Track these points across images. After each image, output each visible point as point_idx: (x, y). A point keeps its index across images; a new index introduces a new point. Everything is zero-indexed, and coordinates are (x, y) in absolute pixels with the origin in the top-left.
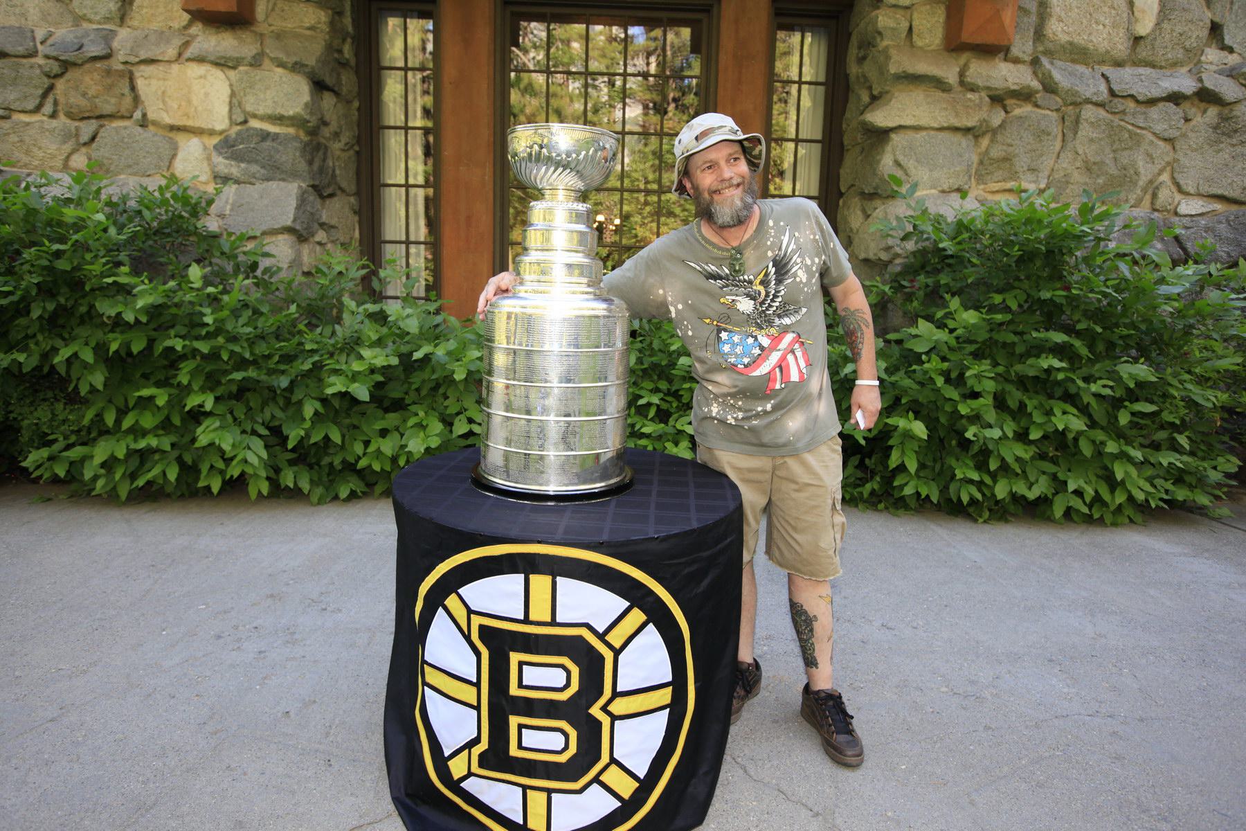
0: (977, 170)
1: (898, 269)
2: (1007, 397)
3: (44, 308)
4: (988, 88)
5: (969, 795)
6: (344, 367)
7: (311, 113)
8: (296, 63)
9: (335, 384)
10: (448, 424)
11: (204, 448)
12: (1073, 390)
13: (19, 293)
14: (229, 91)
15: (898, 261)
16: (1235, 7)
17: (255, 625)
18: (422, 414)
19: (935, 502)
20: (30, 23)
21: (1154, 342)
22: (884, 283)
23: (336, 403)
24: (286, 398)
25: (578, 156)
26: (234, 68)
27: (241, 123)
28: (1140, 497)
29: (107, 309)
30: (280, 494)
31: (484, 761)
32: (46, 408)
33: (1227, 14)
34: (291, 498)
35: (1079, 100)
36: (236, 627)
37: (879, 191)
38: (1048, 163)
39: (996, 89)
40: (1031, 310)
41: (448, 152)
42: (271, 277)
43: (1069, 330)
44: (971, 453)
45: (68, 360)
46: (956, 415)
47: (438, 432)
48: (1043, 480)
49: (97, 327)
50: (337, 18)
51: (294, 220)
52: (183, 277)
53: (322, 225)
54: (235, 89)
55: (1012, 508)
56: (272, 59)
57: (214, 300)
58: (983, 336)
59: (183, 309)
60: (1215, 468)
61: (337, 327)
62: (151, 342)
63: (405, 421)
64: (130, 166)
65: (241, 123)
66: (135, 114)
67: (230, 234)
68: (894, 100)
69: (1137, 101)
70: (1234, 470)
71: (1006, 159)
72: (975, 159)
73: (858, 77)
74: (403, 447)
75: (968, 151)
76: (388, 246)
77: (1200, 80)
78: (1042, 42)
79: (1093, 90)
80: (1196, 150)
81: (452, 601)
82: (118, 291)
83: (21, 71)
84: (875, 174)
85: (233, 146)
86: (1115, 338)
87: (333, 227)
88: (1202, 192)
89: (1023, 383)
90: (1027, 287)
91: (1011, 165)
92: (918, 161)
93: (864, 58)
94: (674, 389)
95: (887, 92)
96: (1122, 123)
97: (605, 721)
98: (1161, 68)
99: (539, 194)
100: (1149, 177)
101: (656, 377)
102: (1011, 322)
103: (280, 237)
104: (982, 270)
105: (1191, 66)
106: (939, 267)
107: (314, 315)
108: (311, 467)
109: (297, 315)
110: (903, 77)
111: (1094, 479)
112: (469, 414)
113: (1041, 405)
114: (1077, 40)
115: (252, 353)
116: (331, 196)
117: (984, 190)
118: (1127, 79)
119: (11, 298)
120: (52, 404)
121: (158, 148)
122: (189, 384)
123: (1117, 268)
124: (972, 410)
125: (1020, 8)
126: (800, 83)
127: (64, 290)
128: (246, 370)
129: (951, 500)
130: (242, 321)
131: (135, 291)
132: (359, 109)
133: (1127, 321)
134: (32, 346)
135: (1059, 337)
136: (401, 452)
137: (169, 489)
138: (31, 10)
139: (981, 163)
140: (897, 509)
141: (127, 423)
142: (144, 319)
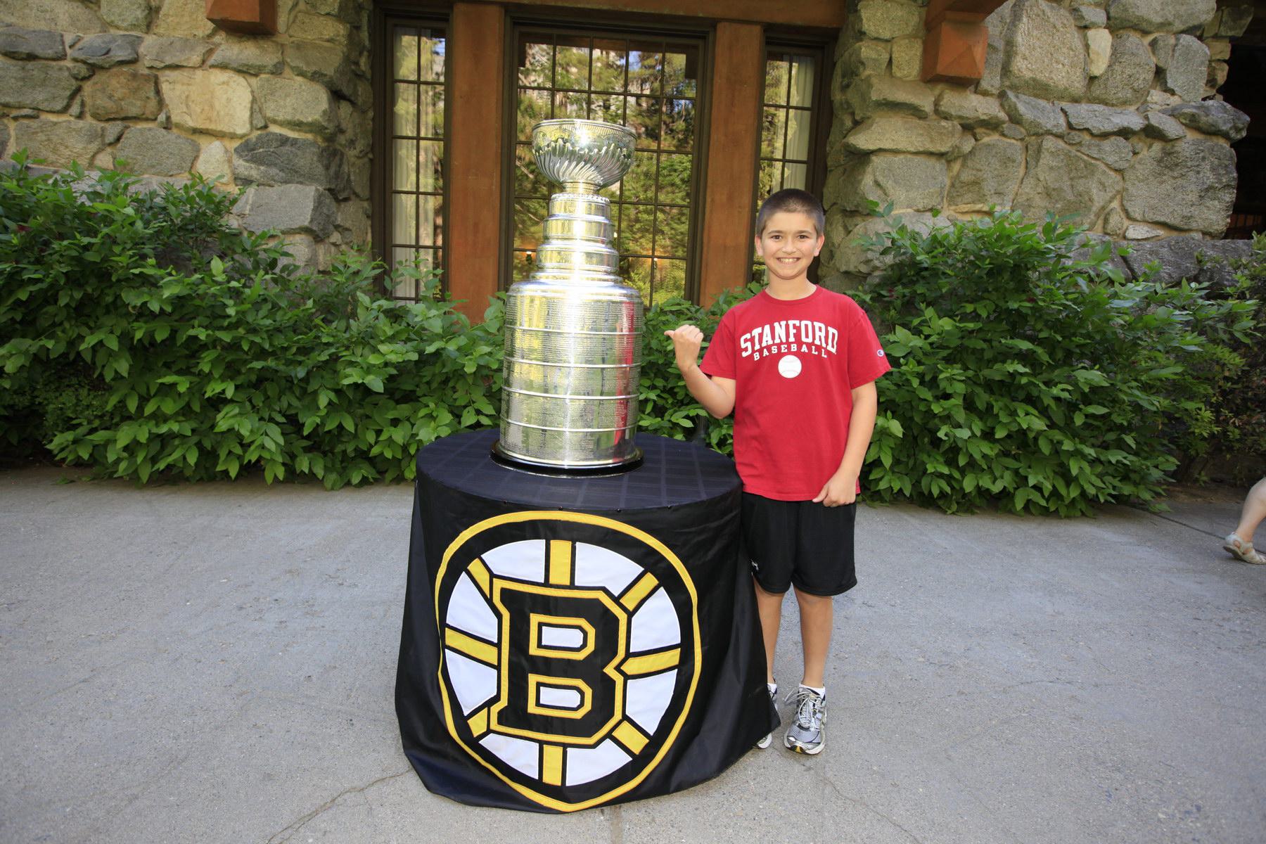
0: (949, 192)
1: (877, 280)
2: (976, 399)
3: (72, 297)
4: (960, 117)
5: (946, 751)
6: (359, 360)
7: (329, 120)
8: (315, 73)
9: (351, 375)
10: (458, 416)
11: (223, 433)
12: (1035, 393)
13: (48, 280)
14: (248, 97)
15: (877, 273)
16: (1177, 54)
17: (275, 597)
18: (432, 405)
19: (908, 495)
20: (59, 28)
21: (1107, 351)
22: (865, 292)
23: (350, 394)
24: (302, 387)
25: (600, 151)
26: (256, 75)
27: (261, 128)
28: (1092, 491)
29: (133, 299)
30: (295, 479)
31: (503, 718)
32: (71, 394)
33: (1170, 60)
34: (306, 483)
35: (1041, 131)
36: (257, 599)
37: (860, 209)
38: (1012, 187)
39: (968, 118)
40: (998, 319)
41: (457, 162)
42: (289, 275)
43: (1032, 339)
44: (942, 450)
45: (93, 347)
46: (929, 414)
47: (448, 422)
48: (1008, 476)
49: (121, 317)
50: (355, 31)
51: (311, 221)
52: (205, 268)
53: (337, 227)
54: (256, 95)
55: (978, 501)
56: (292, 68)
57: (236, 294)
58: (955, 342)
59: (206, 301)
60: (1156, 467)
61: (351, 321)
62: (174, 333)
63: (416, 412)
64: (153, 166)
65: (261, 128)
66: (159, 117)
67: (252, 233)
68: (875, 125)
69: (1092, 135)
70: (1173, 468)
71: (976, 183)
72: (948, 182)
73: (841, 104)
74: (414, 436)
75: (941, 175)
76: (398, 249)
77: (1147, 118)
78: (1008, 78)
79: (1055, 123)
80: (1143, 181)
81: (475, 566)
82: (143, 284)
83: (50, 73)
84: (856, 193)
85: (253, 150)
86: (1072, 347)
87: (347, 229)
88: (1147, 219)
89: (989, 386)
90: (994, 298)
91: (980, 188)
92: (896, 182)
93: (848, 86)
94: (670, 386)
95: (869, 118)
96: (1079, 154)
97: (619, 680)
98: (1113, 105)
99: (561, 187)
100: (1102, 204)
101: (652, 375)
102: (980, 330)
103: (298, 238)
104: (956, 282)
105: (1139, 105)
106: (915, 279)
107: (329, 312)
108: (325, 454)
109: (314, 310)
110: (884, 104)
111: (1051, 475)
112: (477, 406)
113: (1006, 406)
114: (1039, 76)
115: (271, 345)
116: (346, 200)
117: (955, 210)
118: (1084, 114)
119: (39, 286)
120: (77, 390)
121: (181, 150)
122: (210, 372)
123: (1076, 284)
124: (944, 409)
125: (989, 45)
126: (788, 107)
127: (93, 280)
128: (265, 360)
129: (921, 494)
130: (263, 312)
131: (161, 283)
132: (373, 119)
133: (1084, 332)
134: (59, 333)
135: (1025, 345)
136: (412, 441)
137: (188, 473)
138: (61, 16)
139: (953, 185)
140: (873, 501)
141: (149, 409)
142: (168, 309)
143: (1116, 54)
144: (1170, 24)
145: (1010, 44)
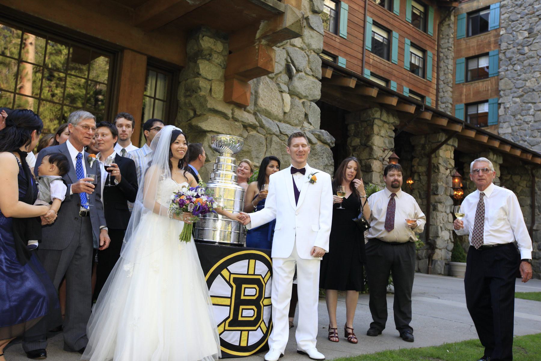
4: (242, 122)
39: (245, 123)
73: (185, 103)
78: (256, 107)
95: (205, 115)
98: (292, 125)
114: (267, 108)
143: (292, 105)
144: (307, 97)
145: (256, 92)
